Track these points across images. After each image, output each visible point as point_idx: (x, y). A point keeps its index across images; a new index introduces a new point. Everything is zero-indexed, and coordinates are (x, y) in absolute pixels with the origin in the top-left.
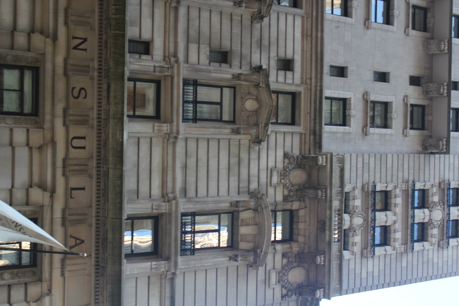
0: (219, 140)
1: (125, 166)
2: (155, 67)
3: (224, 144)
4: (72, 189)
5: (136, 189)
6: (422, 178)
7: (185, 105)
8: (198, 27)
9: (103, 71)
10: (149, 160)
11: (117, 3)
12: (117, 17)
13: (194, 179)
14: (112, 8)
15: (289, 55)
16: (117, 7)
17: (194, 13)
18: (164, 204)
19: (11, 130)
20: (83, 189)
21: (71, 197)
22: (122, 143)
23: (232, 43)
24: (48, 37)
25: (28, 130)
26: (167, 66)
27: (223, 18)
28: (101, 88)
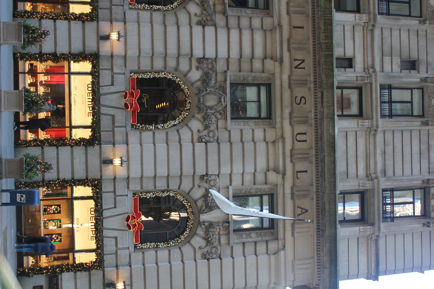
0: (411, 131)
1: (337, 154)
2: (357, 77)
3: (415, 135)
4: (298, 172)
5: (346, 171)
7: (382, 105)
8: (390, 44)
9: (318, 83)
10: (355, 148)
11: (326, 31)
12: (327, 41)
13: (392, 162)
14: (322, 35)
16: (326, 34)
17: (386, 33)
18: (368, 182)
19: (253, 130)
20: (306, 172)
21: (297, 178)
22: (334, 136)
23: (419, 54)
25: (264, 130)
26: (366, 76)
27: (410, 34)
28: (317, 96)
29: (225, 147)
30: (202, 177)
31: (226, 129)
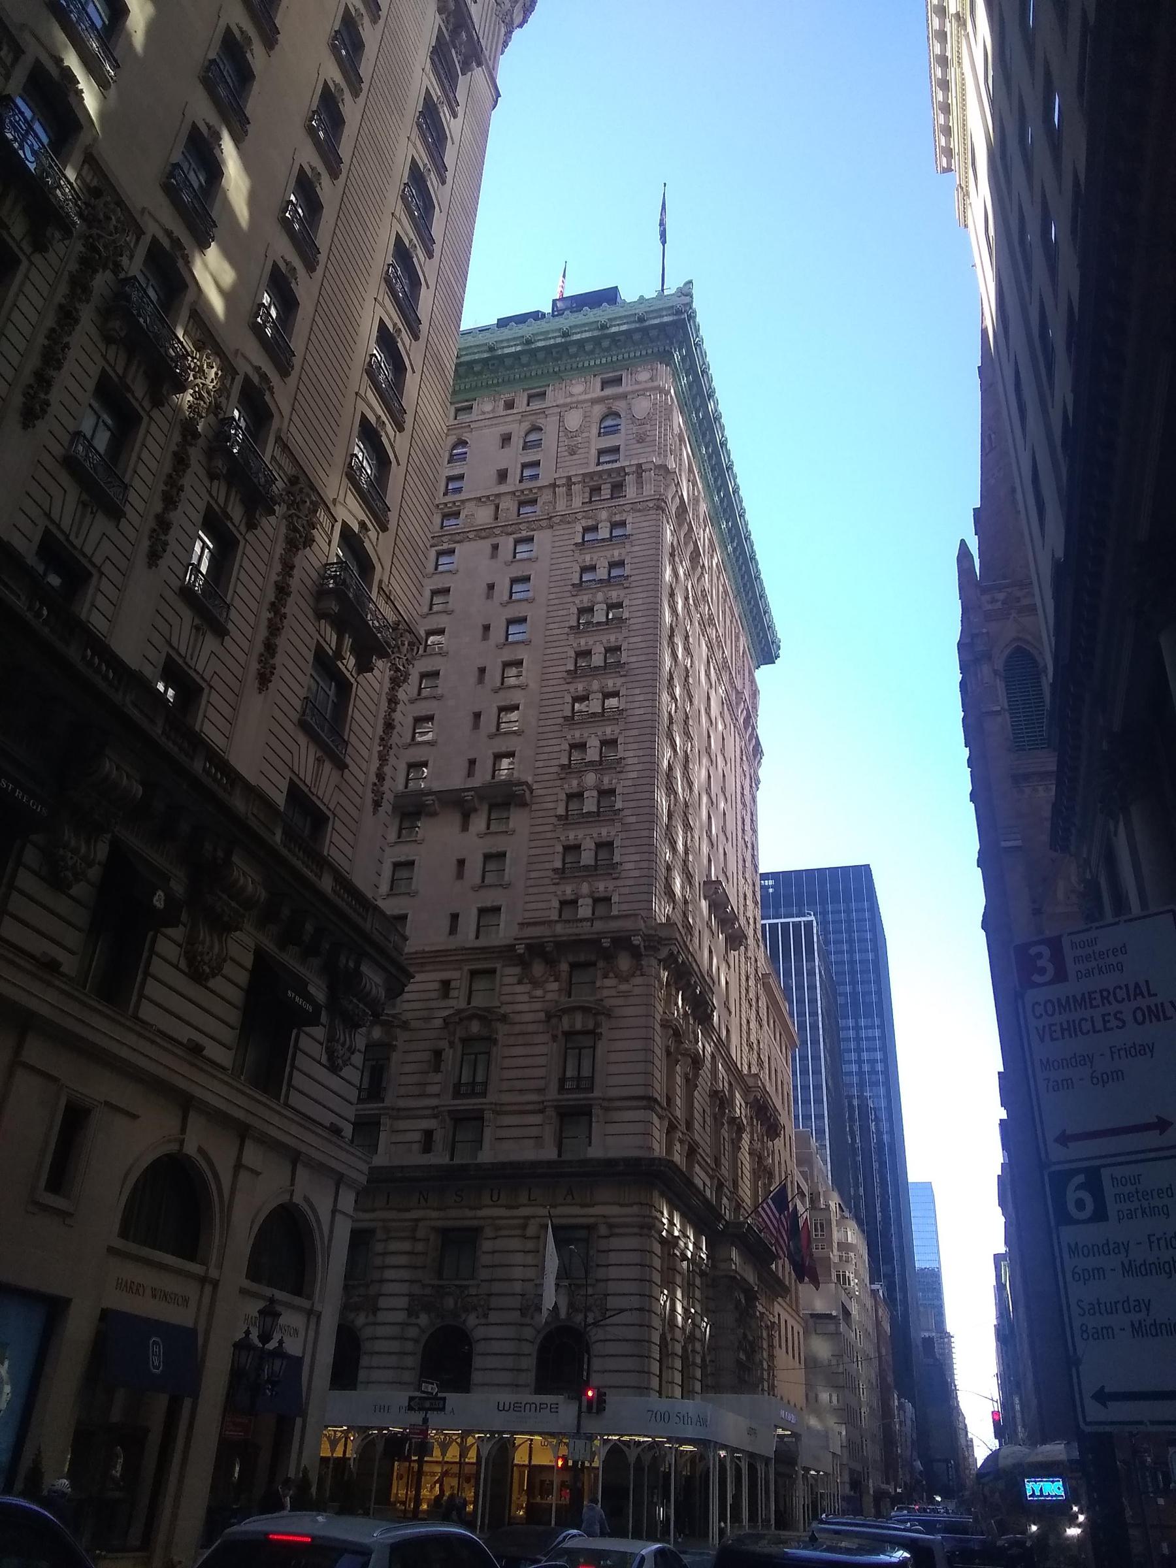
6: (551, 805)
15: (436, 986)
24: (417, 1225)
29: (497, 1287)
30: (523, 1315)
31: (478, 1286)
